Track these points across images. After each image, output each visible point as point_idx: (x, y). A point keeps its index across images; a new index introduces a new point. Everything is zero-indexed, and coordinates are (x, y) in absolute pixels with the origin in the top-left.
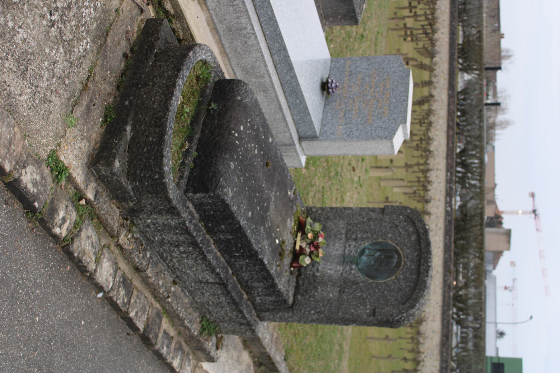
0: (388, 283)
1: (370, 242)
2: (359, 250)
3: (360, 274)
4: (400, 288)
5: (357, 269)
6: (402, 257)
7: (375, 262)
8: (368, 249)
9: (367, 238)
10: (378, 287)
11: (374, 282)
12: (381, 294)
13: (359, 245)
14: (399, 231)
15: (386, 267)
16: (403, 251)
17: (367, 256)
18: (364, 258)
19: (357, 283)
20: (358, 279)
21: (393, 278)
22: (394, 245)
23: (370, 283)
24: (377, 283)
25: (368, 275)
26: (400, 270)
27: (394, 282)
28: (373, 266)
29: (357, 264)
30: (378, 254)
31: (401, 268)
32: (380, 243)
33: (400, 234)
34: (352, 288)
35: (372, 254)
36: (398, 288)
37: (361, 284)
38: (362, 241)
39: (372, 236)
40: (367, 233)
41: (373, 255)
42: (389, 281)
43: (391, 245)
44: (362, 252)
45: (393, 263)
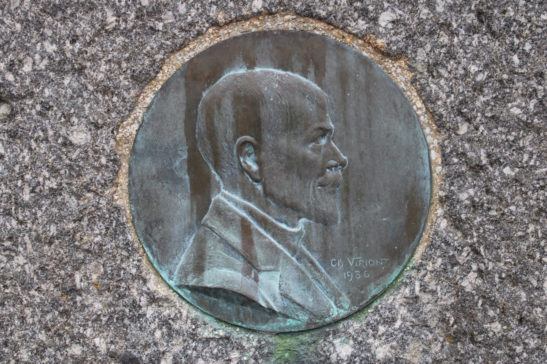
0: (445, 102)
1: (142, 260)
2: (213, 329)
3: (396, 299)
4: (471, 18)
5: (355, 325)
6: (236, 31)
7: (291, 209)
8: (199, 269)
9: (113, 284)
10: (477, 169)
11: (448, 200)
12: (527, 141)
13: (171, 334)
14: (38, 77)
15: (324, 132)
16: (192, 31)
17: (251, 266)
18: (269, 287)
19: (463, 305)
20: (429, 308)
21: (398, 73)
22: (148, 97)
23: (457, 223)
24: (452, 177)
25: (396, 250)
26: (334, 35)
27: (433, 68)
28: (325, 221)
29: (322, 327)
30: (227, 197)
31: (319, 29)
32: (141, 197)
33: (60, 66)
34: (504, 340)
35: (235, 239)
36: (471, 30)
37: (470, 282)
38: (137, 318)
39: (97, 252)
40: (74, 291)
41: (246, 231)
42: (429, 100)
43: (155, 113)
44: (233, 305)
45: (288, 87)
